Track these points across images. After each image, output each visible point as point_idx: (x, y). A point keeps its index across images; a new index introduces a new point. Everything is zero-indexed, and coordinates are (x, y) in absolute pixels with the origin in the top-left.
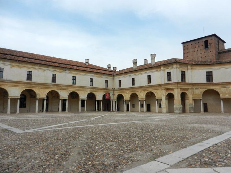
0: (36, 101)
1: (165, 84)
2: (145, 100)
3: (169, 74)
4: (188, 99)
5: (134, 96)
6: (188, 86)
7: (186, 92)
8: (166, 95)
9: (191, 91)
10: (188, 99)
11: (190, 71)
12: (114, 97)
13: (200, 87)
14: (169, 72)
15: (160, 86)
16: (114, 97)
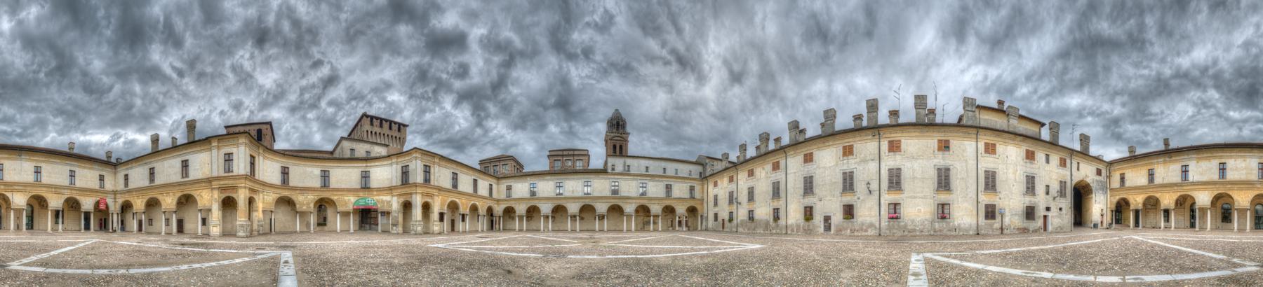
0: (10, 212)
1: (218, 178)
2: (175, 212)
3: (227, 158)
4: (257, 211)
5: (152, 204)
6: (258, 186)
7: (255, 196)
8: (220, 200)
9: (261, 195)
10: (257, 211)
11: (261, 158)
12: (114, 206)
13: (273, 190)
14: (229, 154)
15: (209, 181)
16: (114, 206)
